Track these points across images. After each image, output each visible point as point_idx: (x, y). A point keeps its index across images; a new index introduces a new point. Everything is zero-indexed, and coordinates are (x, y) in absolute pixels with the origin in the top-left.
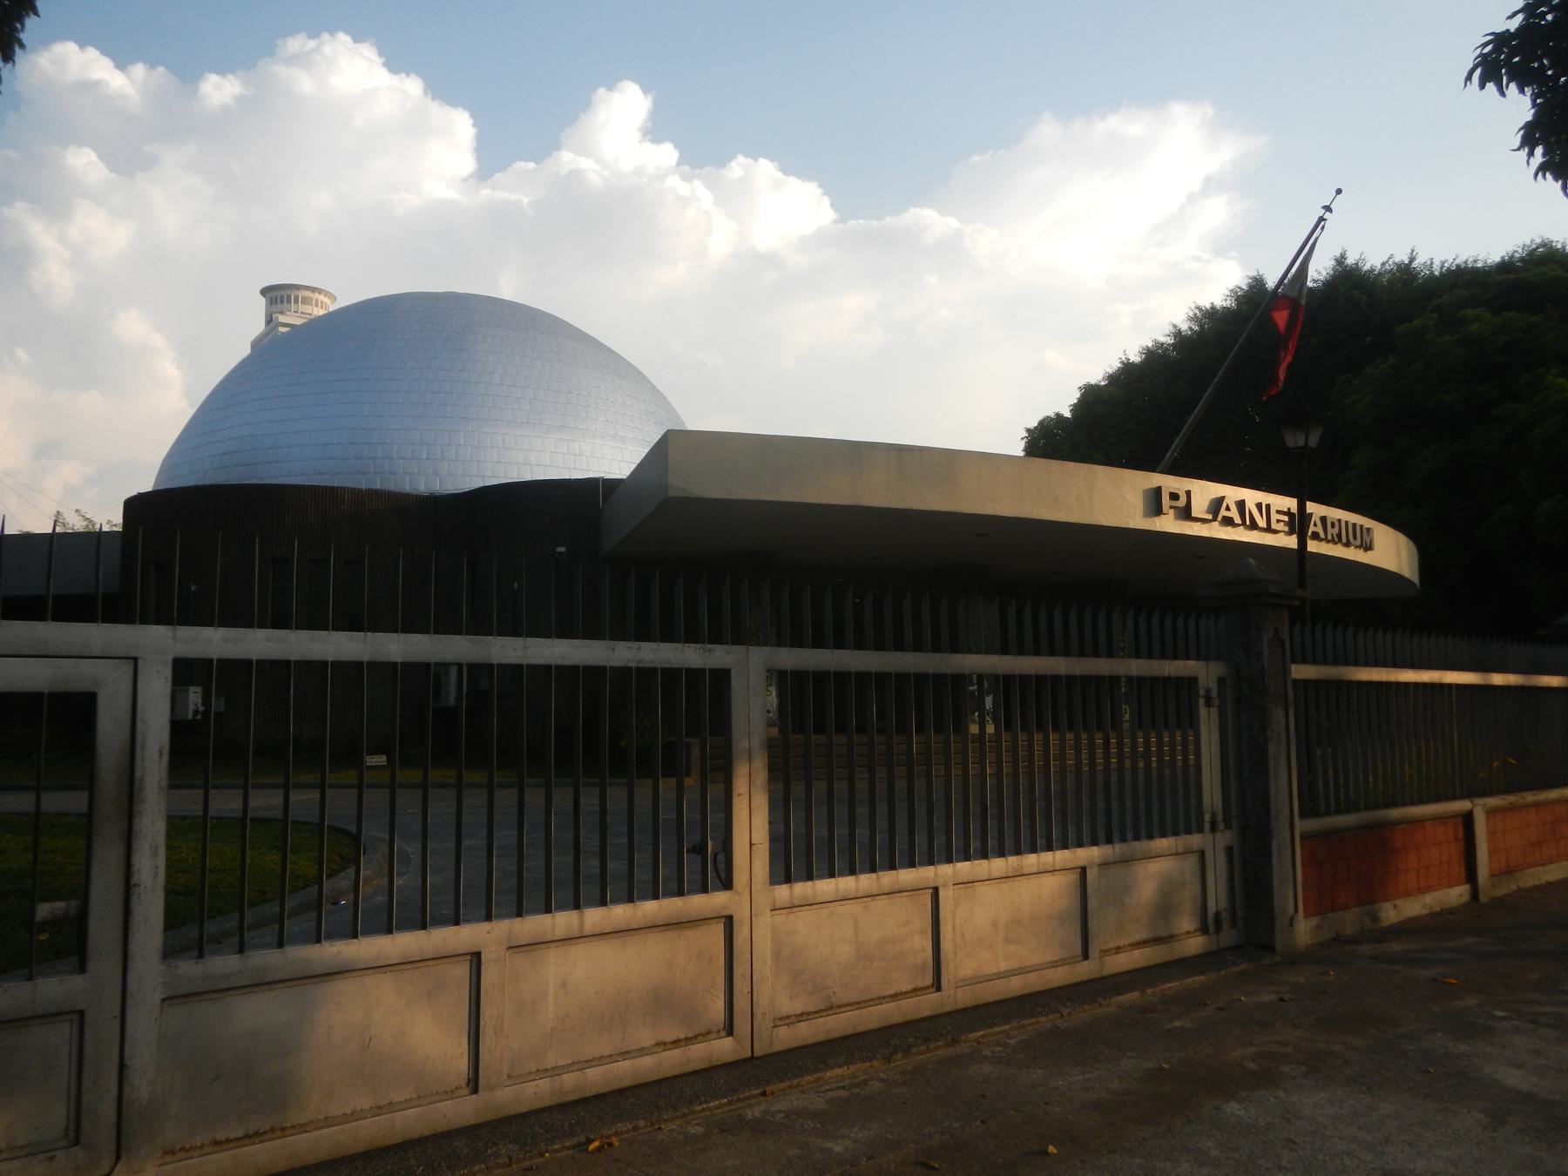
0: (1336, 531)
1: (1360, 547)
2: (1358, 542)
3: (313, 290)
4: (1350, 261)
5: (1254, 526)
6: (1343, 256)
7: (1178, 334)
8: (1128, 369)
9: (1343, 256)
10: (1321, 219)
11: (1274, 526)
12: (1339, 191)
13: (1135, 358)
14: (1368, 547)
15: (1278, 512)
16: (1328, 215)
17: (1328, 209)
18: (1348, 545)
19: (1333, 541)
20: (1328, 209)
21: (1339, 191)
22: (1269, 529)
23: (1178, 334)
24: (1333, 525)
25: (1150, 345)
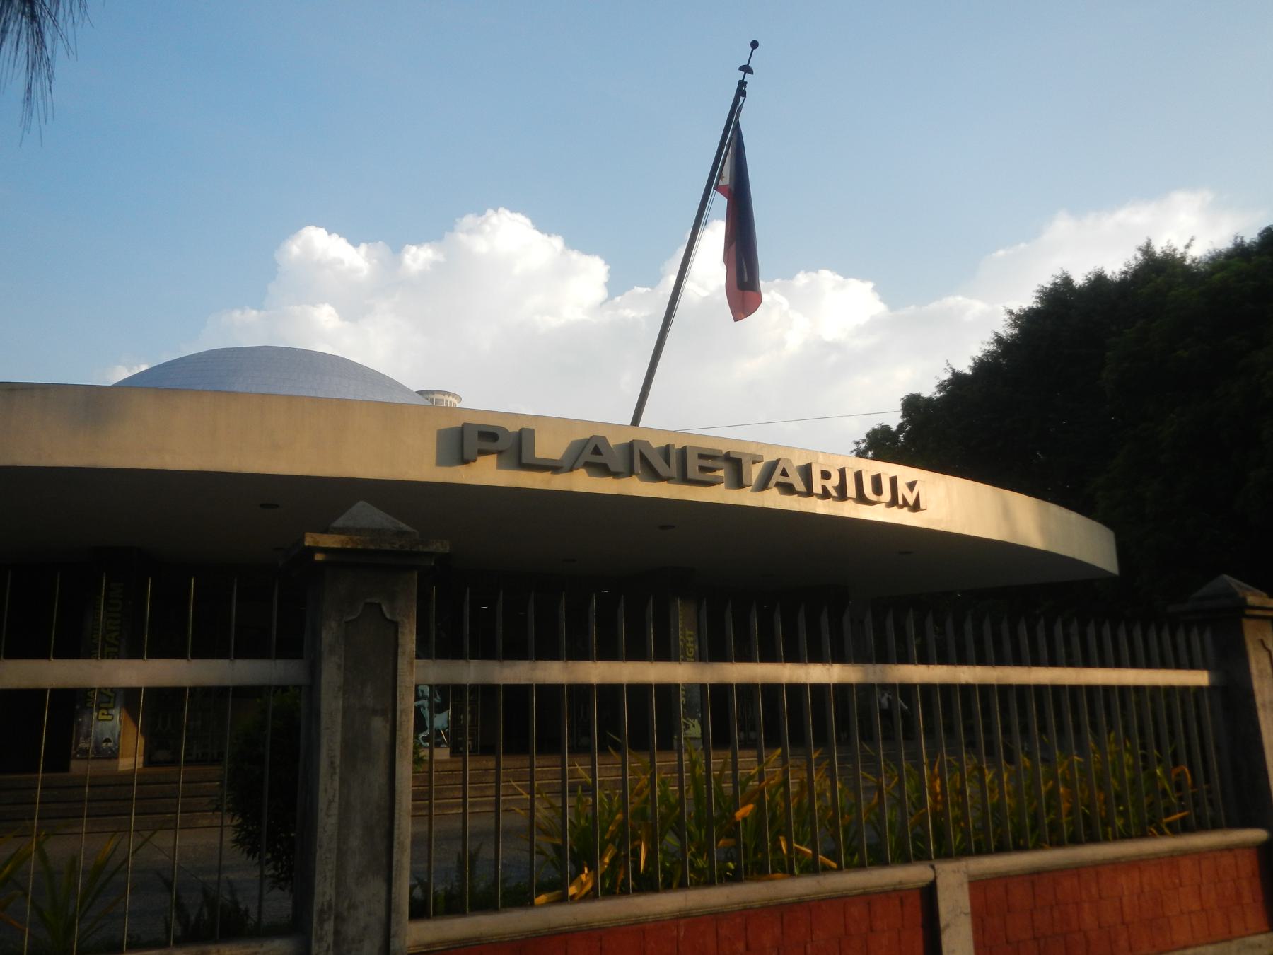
0: (835, 480)
1: (894, 502)
2: (887, 495)
3: (444, 393)
4: (1159, 248)
5: (655, 476)
6: (1148, 245)
7: (999, 341)
8: (958, 379)
9: (1148, 245)
10: (742, 84)
11: (693, 472)
12: (755, 45)
13: (965, 366)
14: (916, 507)
15: (701, 456)
16: (748, 77)
17: (746, 69)
18: (861, 499)
19: (825, 494)
20: (746, 69)
21: (755, 45)
22: (685, 479)
23: (999, 341)
24: (826, 475)
25: (980, 354)
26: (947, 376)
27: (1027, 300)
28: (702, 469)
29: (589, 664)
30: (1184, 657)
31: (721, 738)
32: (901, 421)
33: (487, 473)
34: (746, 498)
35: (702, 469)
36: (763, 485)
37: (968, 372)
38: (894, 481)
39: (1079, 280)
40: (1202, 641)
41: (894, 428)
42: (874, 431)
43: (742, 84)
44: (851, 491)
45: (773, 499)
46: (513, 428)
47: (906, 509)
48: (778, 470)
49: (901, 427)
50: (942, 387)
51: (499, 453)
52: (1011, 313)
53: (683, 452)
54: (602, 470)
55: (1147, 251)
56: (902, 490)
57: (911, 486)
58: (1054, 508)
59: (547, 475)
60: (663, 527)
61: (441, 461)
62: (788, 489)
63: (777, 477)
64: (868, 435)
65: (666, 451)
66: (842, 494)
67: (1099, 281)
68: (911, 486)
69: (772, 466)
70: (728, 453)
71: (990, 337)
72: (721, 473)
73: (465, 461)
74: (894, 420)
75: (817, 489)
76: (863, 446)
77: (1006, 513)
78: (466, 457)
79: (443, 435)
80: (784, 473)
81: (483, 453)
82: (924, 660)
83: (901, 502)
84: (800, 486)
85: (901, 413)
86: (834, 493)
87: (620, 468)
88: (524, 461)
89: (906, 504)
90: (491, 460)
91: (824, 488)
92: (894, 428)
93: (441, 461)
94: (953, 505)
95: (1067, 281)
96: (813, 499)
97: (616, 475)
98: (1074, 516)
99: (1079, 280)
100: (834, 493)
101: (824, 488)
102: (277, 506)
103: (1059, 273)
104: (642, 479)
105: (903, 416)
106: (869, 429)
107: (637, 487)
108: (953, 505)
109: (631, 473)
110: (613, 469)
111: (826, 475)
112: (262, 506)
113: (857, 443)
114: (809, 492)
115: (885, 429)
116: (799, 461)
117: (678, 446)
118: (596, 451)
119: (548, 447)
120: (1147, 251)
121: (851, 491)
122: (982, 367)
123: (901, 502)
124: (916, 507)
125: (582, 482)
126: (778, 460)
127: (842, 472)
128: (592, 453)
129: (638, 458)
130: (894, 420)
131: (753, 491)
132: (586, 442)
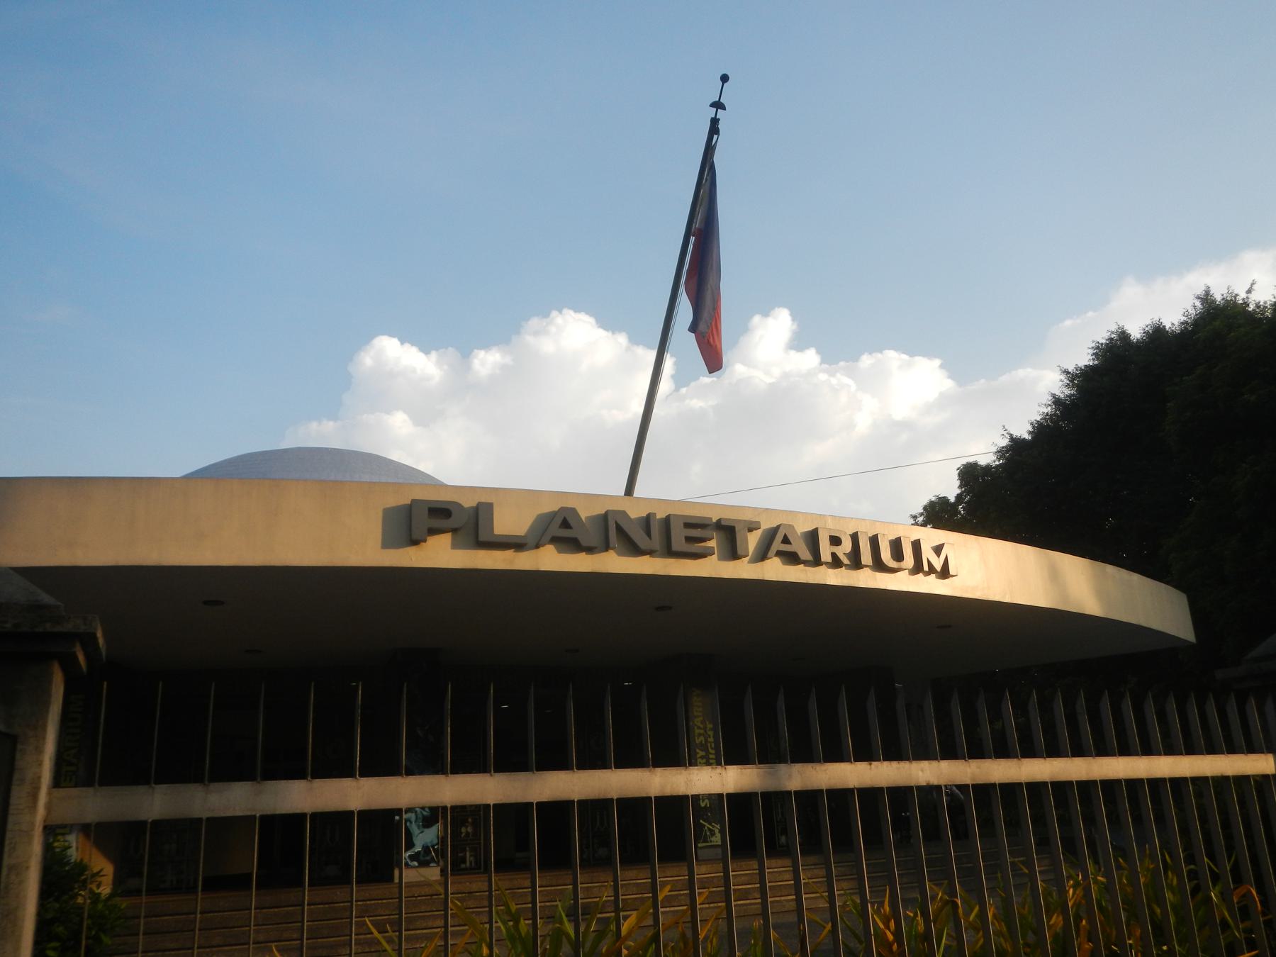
0: (847, 546)
1: (917, 569)
2: (909, 561)
6: (1207, 293)
7: (1057, 401)
8: (1016, 444)
9: (1207, 293)
10: (715, 121)
12: (725, 78)
13: (1023, 431)
14: (945, 573)
15: (688, 525)
17: (718, 105)
18: (879, 566)
19: (836, 563)
20: (718, 105)
21: (725, 78)
22: (670, 553)
23: (1057, 401)
26: (1005, 442)
27: (1083, 358)
28: (689, 540)
29: (347, 783)
30: (1239, 738)
31: (743, 845)
32: (959, 491)
33: (439, 553)
34: (743, 570)
35: (689, 540)
36: (762, 556)
37: (1027, 437)
38: (916, 545)
39: (1136, 333)
40: (1262, 714)
41: (952, 500)
42: (932, 504)
43: (715, 121)
44: (866, 557)
45: (775, 570)
46: (468, 502)
47: (933, 576)
48: (779, 537)
49: (959, 497)
50: (1001, 453)
51: (454, 531)
52: (1066, 372)
53: (667, 521)
54: (572, 544)
55: (1206, 298)
56: (927, 554)
57: (938, 550)
58: (1110, 569)
59: (509, 554)
60: (659, 609)
61: (388, 543)
62: (792, 558)
63: (777, 545)
64: (925, 508)
65: (647, 521)
66: (856, 563)
67: (1157, 334)
68: (938, 550)
69: (773, 533)
70: (719, 521)
71: (1047, 399)
72: (712, 543)
73: (415, 542)
74: (951, 489)
75: (826, 556)
76: (921, 519)
77: (1054, 575)
78: (415, 537)
79: (389, 514)
80: (786, 540)
81: (433, 531)
82: (865, 754)
83: (926, 568)
84: (805, 554)
85: (958, 483)
86: (846, 561)
87: (594, 540)
88: (482, 538)
89: (932, 570)
90: (445, 539)
91: (834, 555)
92: (952, 500)
93: (388, 543)
94: (991, 571)
95: (1124, 335)
96: (823, 568)
97: (590, 550)
98: (1136, 577)
99: (1136, 333)
100: (846, 561)
101: (834, 555)
102: (222, 603)
103: (1114, 328)
104: (621, 554)
105: (960, 487)
106: (925, 502)
107: (614, 563)
108: (991, 571)
109: (607, 548)
110: (584, 543)
111: (835, 541)
112: (206, 603)
113: (915, 517)
114: (817, 561)
115: (943, 501)
116: (802, 527)
117: (661, 515)
118: (565, 524)
119: (507, 523)
120: (1206, 298)
121: (866, 557)
122: (1041, 430)
123: (926, 568)
124: (945, 573)
125: (550, 560)
126: (779, 527)
127: (855, 538)
128: (562, 527)
129: (614, 530)
130: (951, 489)
131: (750, 562)
132: (553, 515)
